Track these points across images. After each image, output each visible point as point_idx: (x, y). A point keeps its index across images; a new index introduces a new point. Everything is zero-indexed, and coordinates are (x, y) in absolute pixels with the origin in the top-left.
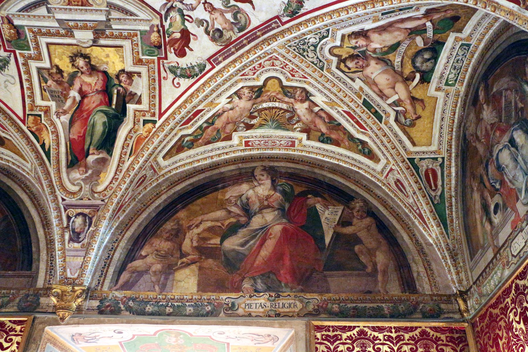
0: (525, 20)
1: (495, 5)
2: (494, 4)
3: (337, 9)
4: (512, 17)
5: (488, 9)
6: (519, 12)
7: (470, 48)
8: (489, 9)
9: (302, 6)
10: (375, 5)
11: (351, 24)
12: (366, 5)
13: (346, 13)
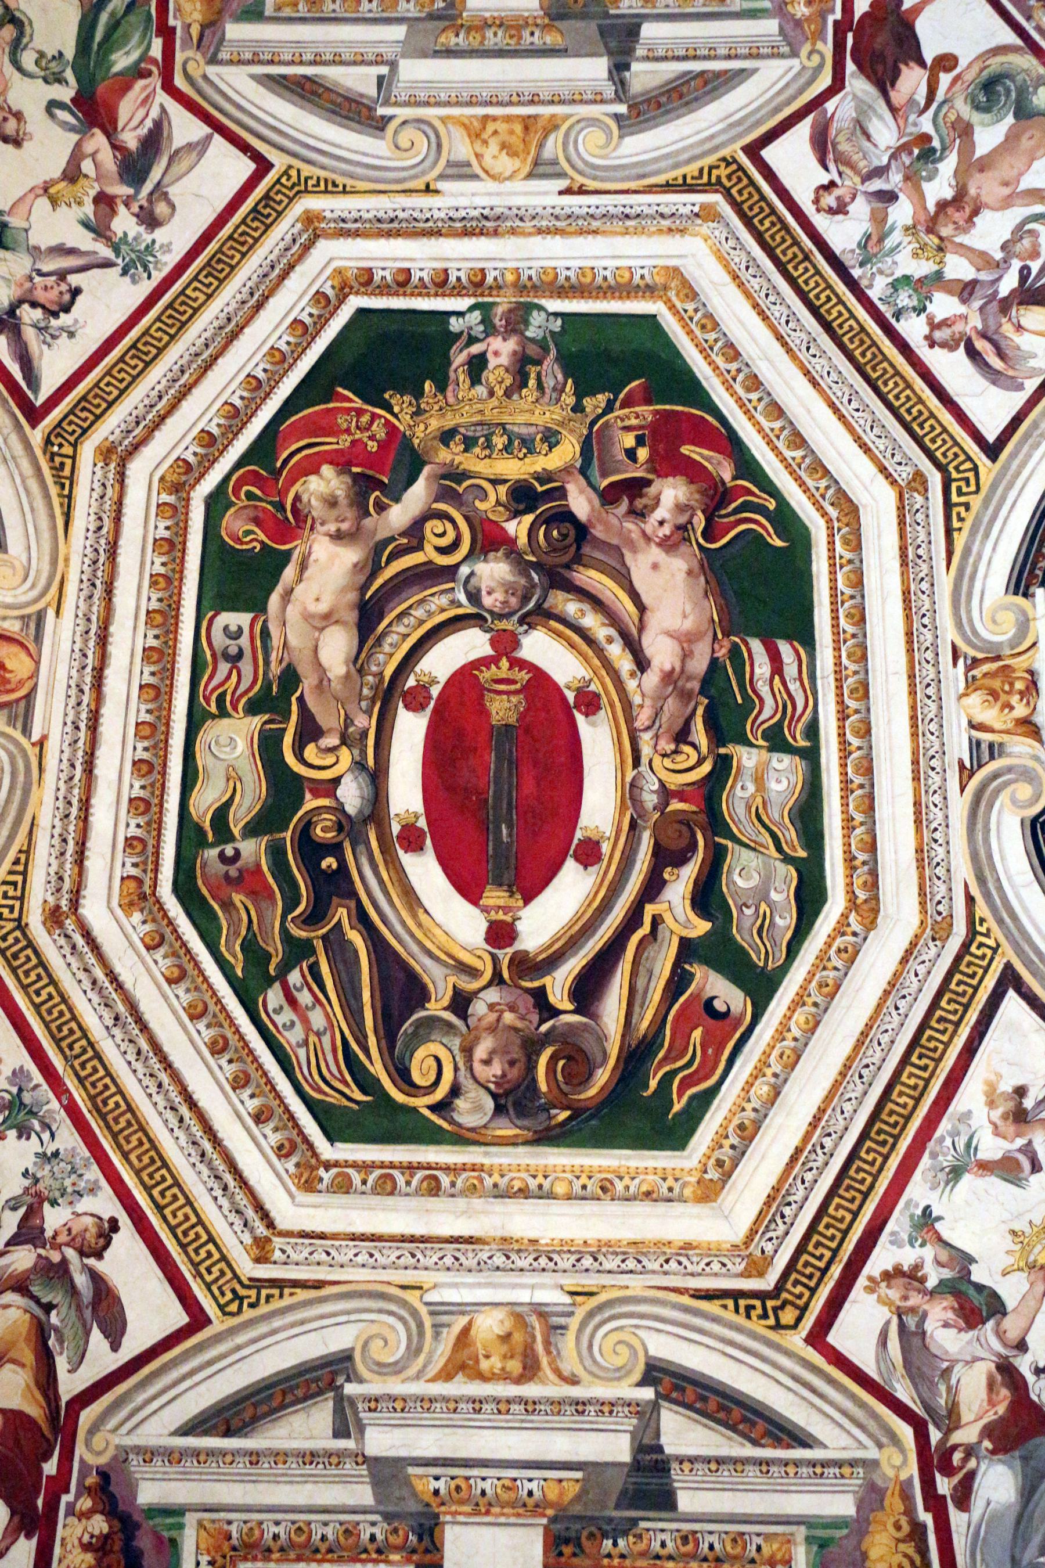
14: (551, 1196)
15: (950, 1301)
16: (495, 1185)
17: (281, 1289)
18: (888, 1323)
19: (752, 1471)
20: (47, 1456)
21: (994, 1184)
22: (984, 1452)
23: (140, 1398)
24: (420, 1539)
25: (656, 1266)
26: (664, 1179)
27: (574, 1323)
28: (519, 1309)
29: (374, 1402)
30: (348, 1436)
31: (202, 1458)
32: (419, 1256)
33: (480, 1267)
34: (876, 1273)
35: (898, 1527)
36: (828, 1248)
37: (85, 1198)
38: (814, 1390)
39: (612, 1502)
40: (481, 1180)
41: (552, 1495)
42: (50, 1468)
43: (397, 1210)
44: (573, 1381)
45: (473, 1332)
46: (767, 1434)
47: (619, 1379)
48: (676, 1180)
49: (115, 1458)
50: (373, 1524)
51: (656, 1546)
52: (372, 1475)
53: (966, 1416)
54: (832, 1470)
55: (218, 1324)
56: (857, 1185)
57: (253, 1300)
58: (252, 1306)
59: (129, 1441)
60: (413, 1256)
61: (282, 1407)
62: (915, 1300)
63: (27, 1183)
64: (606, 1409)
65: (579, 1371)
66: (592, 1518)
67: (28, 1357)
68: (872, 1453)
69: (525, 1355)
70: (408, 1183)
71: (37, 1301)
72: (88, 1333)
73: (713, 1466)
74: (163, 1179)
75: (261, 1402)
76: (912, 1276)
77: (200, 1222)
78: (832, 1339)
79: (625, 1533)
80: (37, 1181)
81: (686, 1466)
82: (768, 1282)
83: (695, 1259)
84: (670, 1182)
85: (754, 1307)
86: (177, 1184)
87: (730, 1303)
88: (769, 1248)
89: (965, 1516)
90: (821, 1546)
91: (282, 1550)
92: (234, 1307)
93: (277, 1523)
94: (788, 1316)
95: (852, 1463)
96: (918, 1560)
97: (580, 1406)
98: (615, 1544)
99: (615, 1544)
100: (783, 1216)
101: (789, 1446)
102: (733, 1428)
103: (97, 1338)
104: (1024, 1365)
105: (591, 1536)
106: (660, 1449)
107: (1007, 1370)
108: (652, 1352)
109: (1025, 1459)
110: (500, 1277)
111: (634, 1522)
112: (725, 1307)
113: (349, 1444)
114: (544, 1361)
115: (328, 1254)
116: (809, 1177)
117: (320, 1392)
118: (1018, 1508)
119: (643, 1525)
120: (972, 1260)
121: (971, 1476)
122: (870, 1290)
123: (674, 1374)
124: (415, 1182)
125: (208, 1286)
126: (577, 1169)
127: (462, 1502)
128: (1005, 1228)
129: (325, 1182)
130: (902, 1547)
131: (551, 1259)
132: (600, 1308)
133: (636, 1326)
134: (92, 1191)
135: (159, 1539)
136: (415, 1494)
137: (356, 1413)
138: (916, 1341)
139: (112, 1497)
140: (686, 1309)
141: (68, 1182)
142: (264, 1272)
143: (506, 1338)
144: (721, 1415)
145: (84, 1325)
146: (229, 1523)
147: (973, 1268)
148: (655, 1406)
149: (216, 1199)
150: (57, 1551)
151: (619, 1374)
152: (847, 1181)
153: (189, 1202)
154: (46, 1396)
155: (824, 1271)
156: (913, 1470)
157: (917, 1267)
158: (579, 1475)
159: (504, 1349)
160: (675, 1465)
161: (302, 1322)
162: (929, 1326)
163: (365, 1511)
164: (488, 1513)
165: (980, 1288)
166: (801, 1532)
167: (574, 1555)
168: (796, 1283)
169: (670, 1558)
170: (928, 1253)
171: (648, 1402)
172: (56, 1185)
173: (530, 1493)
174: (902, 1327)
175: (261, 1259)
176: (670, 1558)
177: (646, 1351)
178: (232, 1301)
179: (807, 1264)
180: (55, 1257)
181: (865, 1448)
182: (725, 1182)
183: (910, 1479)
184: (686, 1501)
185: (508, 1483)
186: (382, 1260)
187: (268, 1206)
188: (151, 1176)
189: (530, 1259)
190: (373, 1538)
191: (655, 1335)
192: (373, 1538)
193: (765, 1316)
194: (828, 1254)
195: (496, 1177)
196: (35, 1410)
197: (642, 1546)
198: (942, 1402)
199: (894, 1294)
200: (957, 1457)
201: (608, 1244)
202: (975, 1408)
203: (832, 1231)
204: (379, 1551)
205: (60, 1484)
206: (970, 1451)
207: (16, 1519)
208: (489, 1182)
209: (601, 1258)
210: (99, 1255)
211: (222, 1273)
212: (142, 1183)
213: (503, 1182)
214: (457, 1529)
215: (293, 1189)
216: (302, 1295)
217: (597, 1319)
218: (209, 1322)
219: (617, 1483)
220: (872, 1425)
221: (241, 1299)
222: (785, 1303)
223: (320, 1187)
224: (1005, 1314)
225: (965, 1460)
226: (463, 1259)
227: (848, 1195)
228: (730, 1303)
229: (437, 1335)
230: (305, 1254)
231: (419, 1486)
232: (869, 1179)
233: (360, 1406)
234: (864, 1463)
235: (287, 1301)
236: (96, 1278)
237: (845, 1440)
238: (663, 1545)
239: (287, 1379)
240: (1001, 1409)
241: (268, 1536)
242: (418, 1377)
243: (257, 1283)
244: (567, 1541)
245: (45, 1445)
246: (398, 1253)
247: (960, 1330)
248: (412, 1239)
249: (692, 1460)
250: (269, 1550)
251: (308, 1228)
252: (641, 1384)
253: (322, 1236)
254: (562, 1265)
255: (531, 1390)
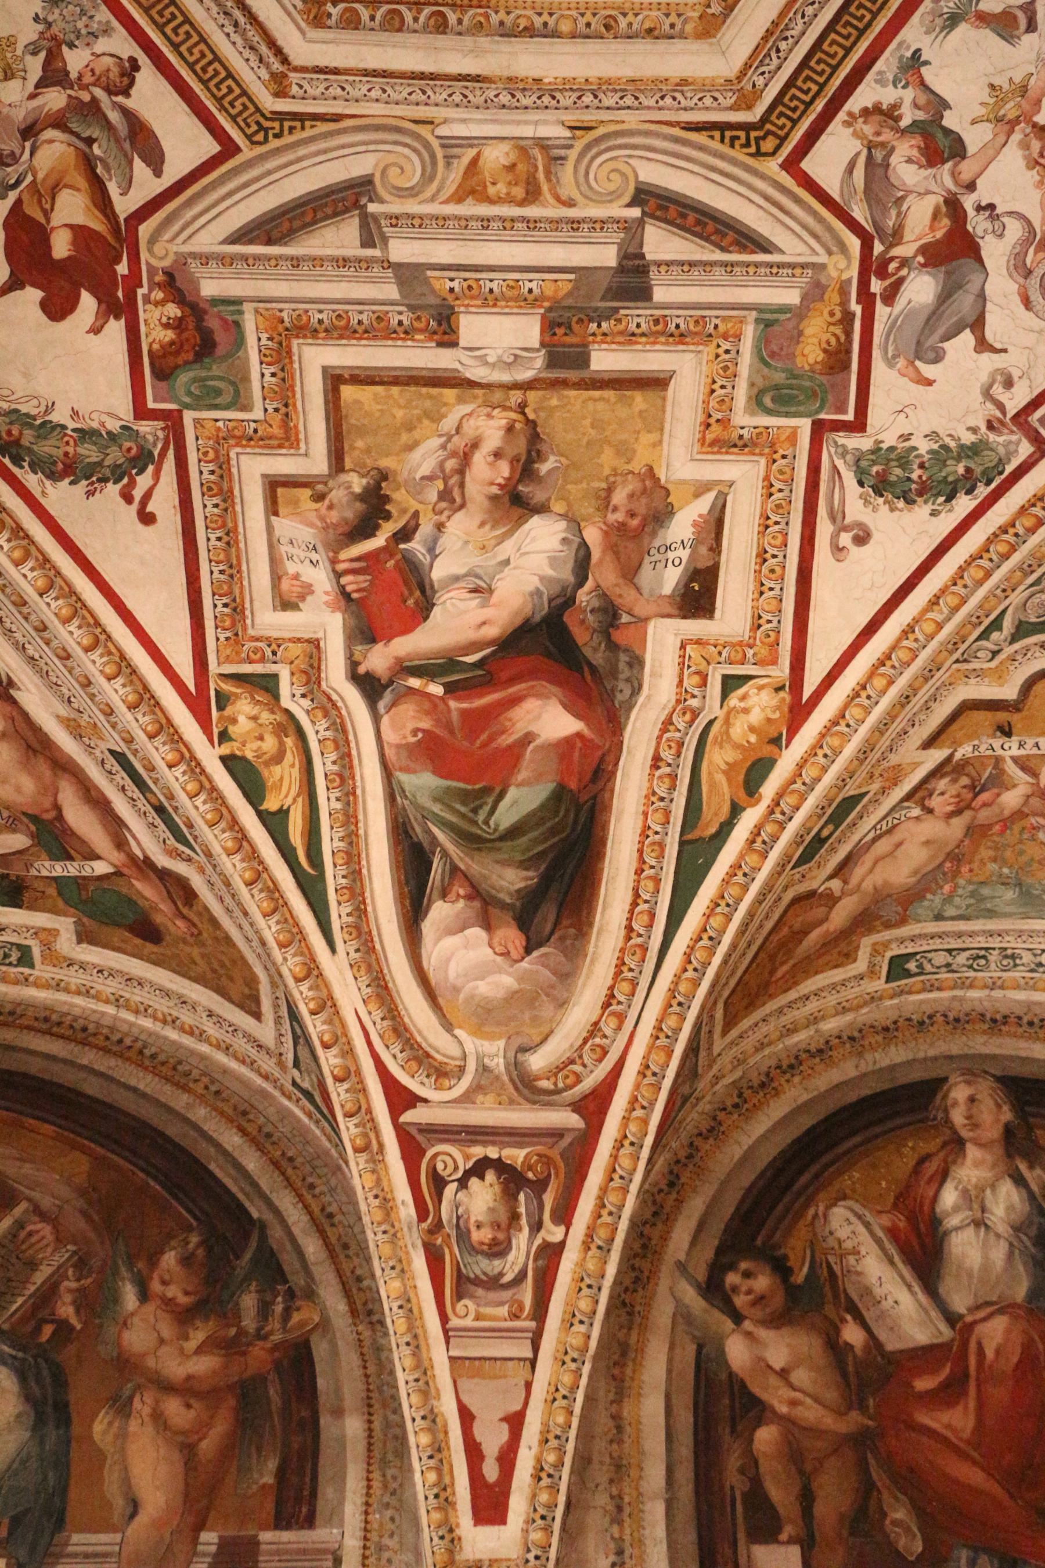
0: (400, 1261)
1: (374, 1142)
2: (372, 1135)
3: (84, 605)
4: (378, 1216)
5: (351, 1125)
6: (405, 1229)
7: (16, 966)
8: (354, 1131)
9: (54, 476)
10: (161, 738)
11: (31, 651)
12: (143, 708)
13: (85, 642)
14: (556, 34)
15: (918, 140)
16: (502, 23)
17: (302, 121)
18: (858, 154)
19: (718, 271)
20: (118, 260)
21: (988, 37)
22: (916, 265)
23: (189, 214)
24: (440, 324)
25: (652, 102)
26: (667, 15)
27: (573, 154)
28: (523, 143)
29: (395, 219)
30: (374, 246)
31: (251, 261)
32: (430, 92)
33: (487, 104)
34: (856, 110)
35: (832, 314)
36: (816, 82)
37: (101, 39)
38: (781, 208)
39: (600, 295)
40: (487, 16)
41: (549, 292)
42: (122, 269)
43: (405, 47)
44: (570, 203)
45: (481, 162)
46: (737, 243)
47: (611, 201)
48: (679, 15)
49: (175, 261)
50: (400, 313)
51: (633, 327)
52: (396, 276)
53: (908, 236)
54: (785, 271)
55: (248, 152)
56: (855, 22)
57: (277, 131)
58: (277, 136)
59: (186, 249)
60: (424, 92)
61: (314, 222)
62: (887, 136)
63: (40, 27)
64: (598, 226)
65: (576, 195)
66: (582, 308)
67: (82, 182)
68: (822, 258)
69: (528, 183)
70: (416, 20)
71: (77, 135)
72: (130, 163)
73: (686, 268)
74: (174, 17)
75: (294, 218)
76: (887, 114)
77: (217, 58)
78: (804, 165)
79: (608, 318)
80: (49, 25)
81: (663, 269)
82: (753, 116)
83: (689, 95)
84: (673, 18)
85: (738, 138)
86: (187, 20)
87: (717, 134)
88: (760, 81)
89: (888, 309)
90: (766, 326)
91: (326, 330)
92: (260, 137)
93: (320, 311)
94: (768, 145)
95: (803, 266)
96: (843, 338)
97: (575, 224)
98: (599, 326)
99: (599, 326)
100: (778, 51)
101: (753, 252)
102: (707, 239)
103: (139, 166)
104: (969, 202)
105: (580, 321)
106: (642, 256)
107: (953, 206)
108: (641, 178)
109: (948, 273)
110: (504, 115)
111: (616, 310)
112: (712, 137)
113: (376, 253)
114: (545, 188)
115: (343, 89)
116: (810, 11)
117: (346, 210)
118: (932, 308)
119: (622, 312)
120: (945, 105)
121: (901, 281)
122: (847, 124)
123: (659, 196)
124: (422, 19)
125: (234, 119)
126: (582, 6)
127: (473, 298)
128: (987, 81)
129: (334, 18)
130: (832, 328)
131: (554, 98)
132: (598, 141)
133: (630, 156)
134: (107, 31)
135: (225, 321)
136: (433, 291)
137: (379, 227)
138: (880, 172)
139: (179, 290)
140: (677, 140)
141: (80, 24)
142: (283, 105)
143: (511, 168)
144: (697, 229)
145: (126, 155)
146: (281, 311)
147: (947, 113)
148: (641, 223)
149: (228, 35)
150: (143, 329)
151: (612, 197)
152: (846, 17)
153: (203, 40)
154: (106, 216)
155: (808, 105)
156: (854, 272)
157: (895, 106)
158: (572, 277)
159: (510, 177)
160: (653, 268)
161: (325, 152)
162: (894, 160)
163: (392, 303)
164: (495, 305)
165: (947, 132)
166: (754, 314)
167: (566, 334)
168: (781, 114)
169: (643, 335)
170: (908, 95)
171: (634, 220)
172: (69, 27)
173: (530, 291)
174: (870, 157)
175: (281, 93)
176: (643, 335)
177: (636, 176)
178: (256, 132)
179: (794, 97)
180: (86, 97)
181: (817, 254)
182: (726, 16)
183: (849, 281)
184: (660, 294)
185: (512, 283)
186: (395, 96)
187: (280, 42)
188: (160, 13)
189: (534, 98)
190: (400, 323)
191: (644, 162)
192: (400, 323)
193: (748, 145)
194: (815, 88)
195: (502, 15)
196: (98, 225)
197: (621, 327)
198: (891, 224)
199: (868, 130)
200: (892, 266)
201: (609, 82)
202: (917, 231)
203: (822, 66)
204: (406, 332)
205: (133, 280)
206: (904, 262)
207: (104, 306)
208: (495, 19)
209: (601, 96)
210: (126, 92)
211: (245, 108)
212: (154, 22)
213: (509, 20)
214: (470, 317)
215: (303, 24)
216: (323, 127)
217: (594, 151)
218: (238, 150)
219: (604, 282)
220: (826, 237)
221: (266, 130)
222: (769, 133)
223: (329, 23)
224: (964, 157)
225: (899, 269)
226: (471, 97)
227: (844, 31)
228: (717, 134)
229: (448, 164)
230: (321, 89)
231: (437, 285)
232: (868, 17)
233: (383, 222)
234: (813, 266)
235: (308, 133)
236: (128, 114)
237: (801, 248)
238: (638, 326)
239: (316, 199)
240: (939, 235)
241: (314, 321)
242: (433, 199)
243: (280, 116)
244: (560, 325)
245: (114, 253)
246: (410, 90)
247: (921, 167)
248: (422, 76)
249: (668, 264)
250: (316, 331)
251: (322, 63)
252: (629, 205)
253: (336, 71)
254: (564, 102)
255: (532, 211)
